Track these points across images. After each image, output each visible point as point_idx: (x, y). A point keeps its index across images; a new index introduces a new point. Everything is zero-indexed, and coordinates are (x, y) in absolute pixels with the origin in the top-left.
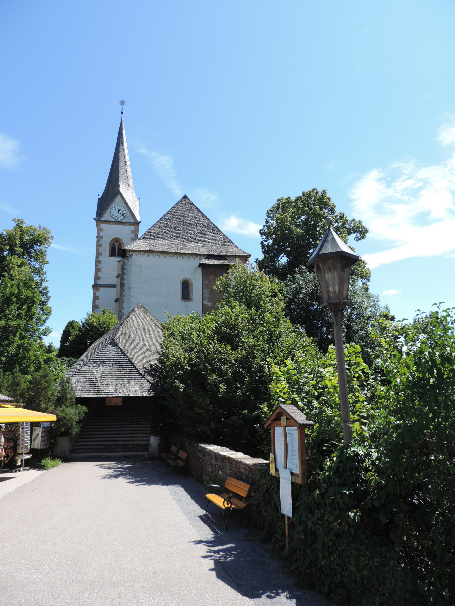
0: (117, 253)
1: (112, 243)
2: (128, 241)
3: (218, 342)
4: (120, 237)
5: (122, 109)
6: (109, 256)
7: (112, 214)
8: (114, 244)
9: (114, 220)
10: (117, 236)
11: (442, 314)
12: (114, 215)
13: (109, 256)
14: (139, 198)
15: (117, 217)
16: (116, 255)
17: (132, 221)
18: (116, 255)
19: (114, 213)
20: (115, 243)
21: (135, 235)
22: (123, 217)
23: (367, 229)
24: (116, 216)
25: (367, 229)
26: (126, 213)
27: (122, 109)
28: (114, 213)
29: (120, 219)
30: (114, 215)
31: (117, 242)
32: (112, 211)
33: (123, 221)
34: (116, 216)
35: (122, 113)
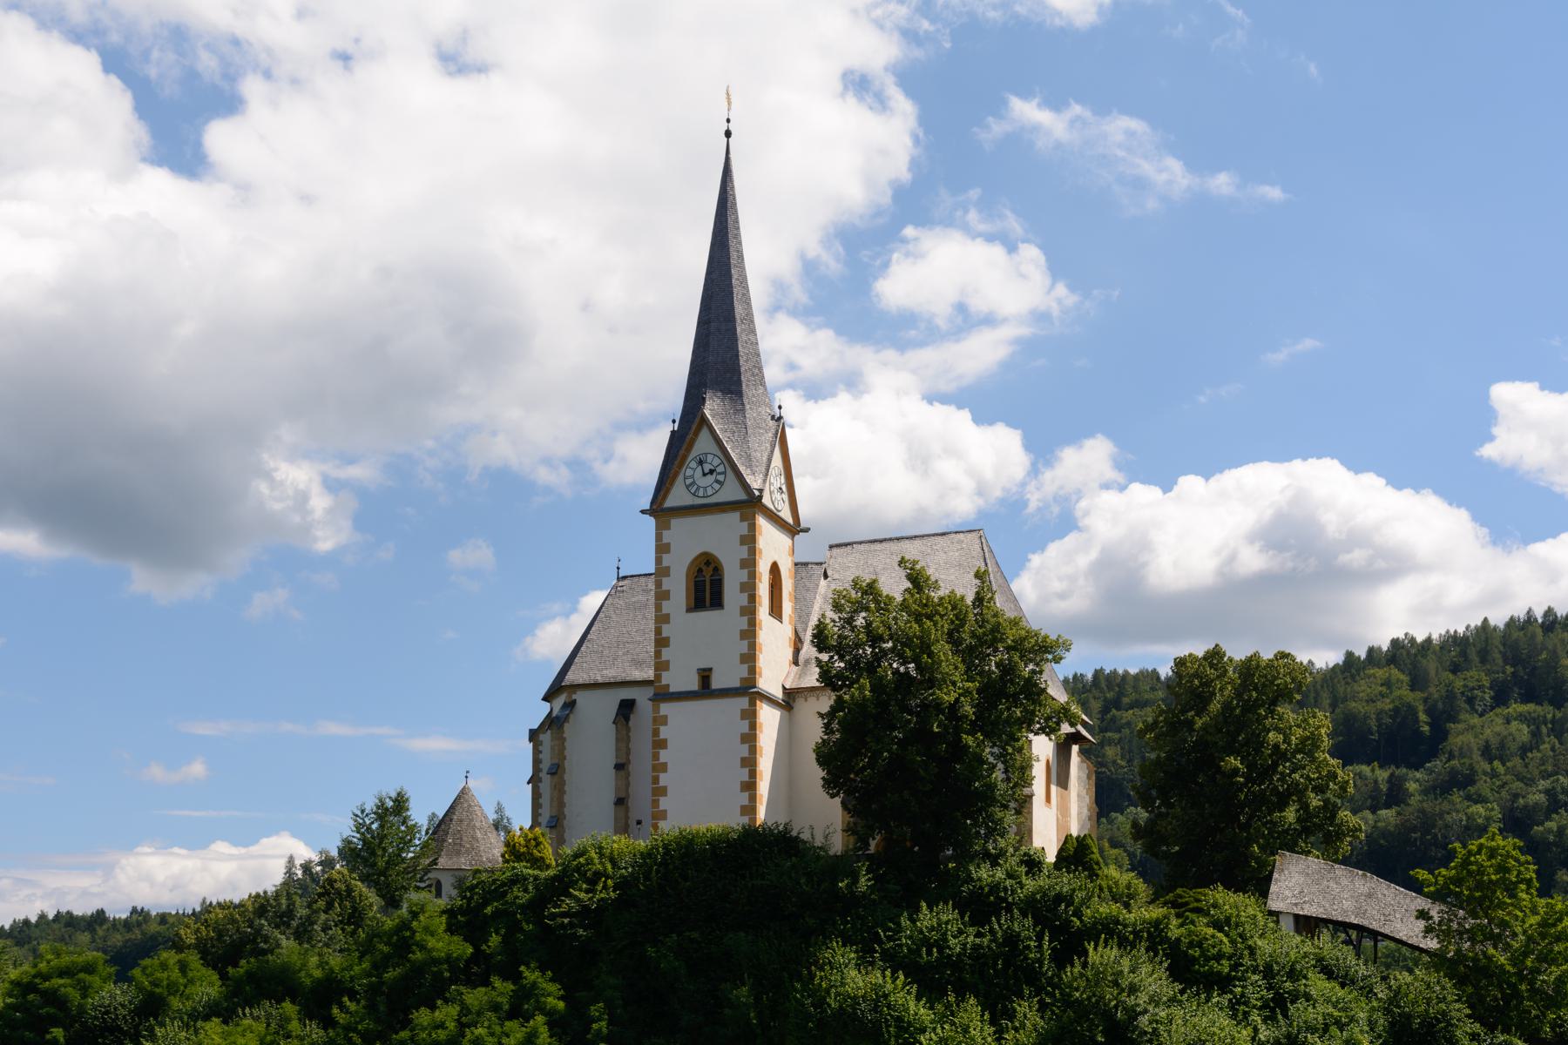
3: (1328, 771)
5: (728, 121)
6: (689, 610)
7: (689, 481)
11: (1480, 753)
12: (694, 483)
13: (689, 610)
14: (780, 407)
15: (701, 489)
19: (692, 477)
22: (717, 486)
23: (142, 909)
24: (698, 488)
25: (142, 909)
26: (724, 473)
27: (728, 121)
28: (692, 477)
30: (694, 483)
31: (708, 563)
32: (689, 472)
35: (728, 134)
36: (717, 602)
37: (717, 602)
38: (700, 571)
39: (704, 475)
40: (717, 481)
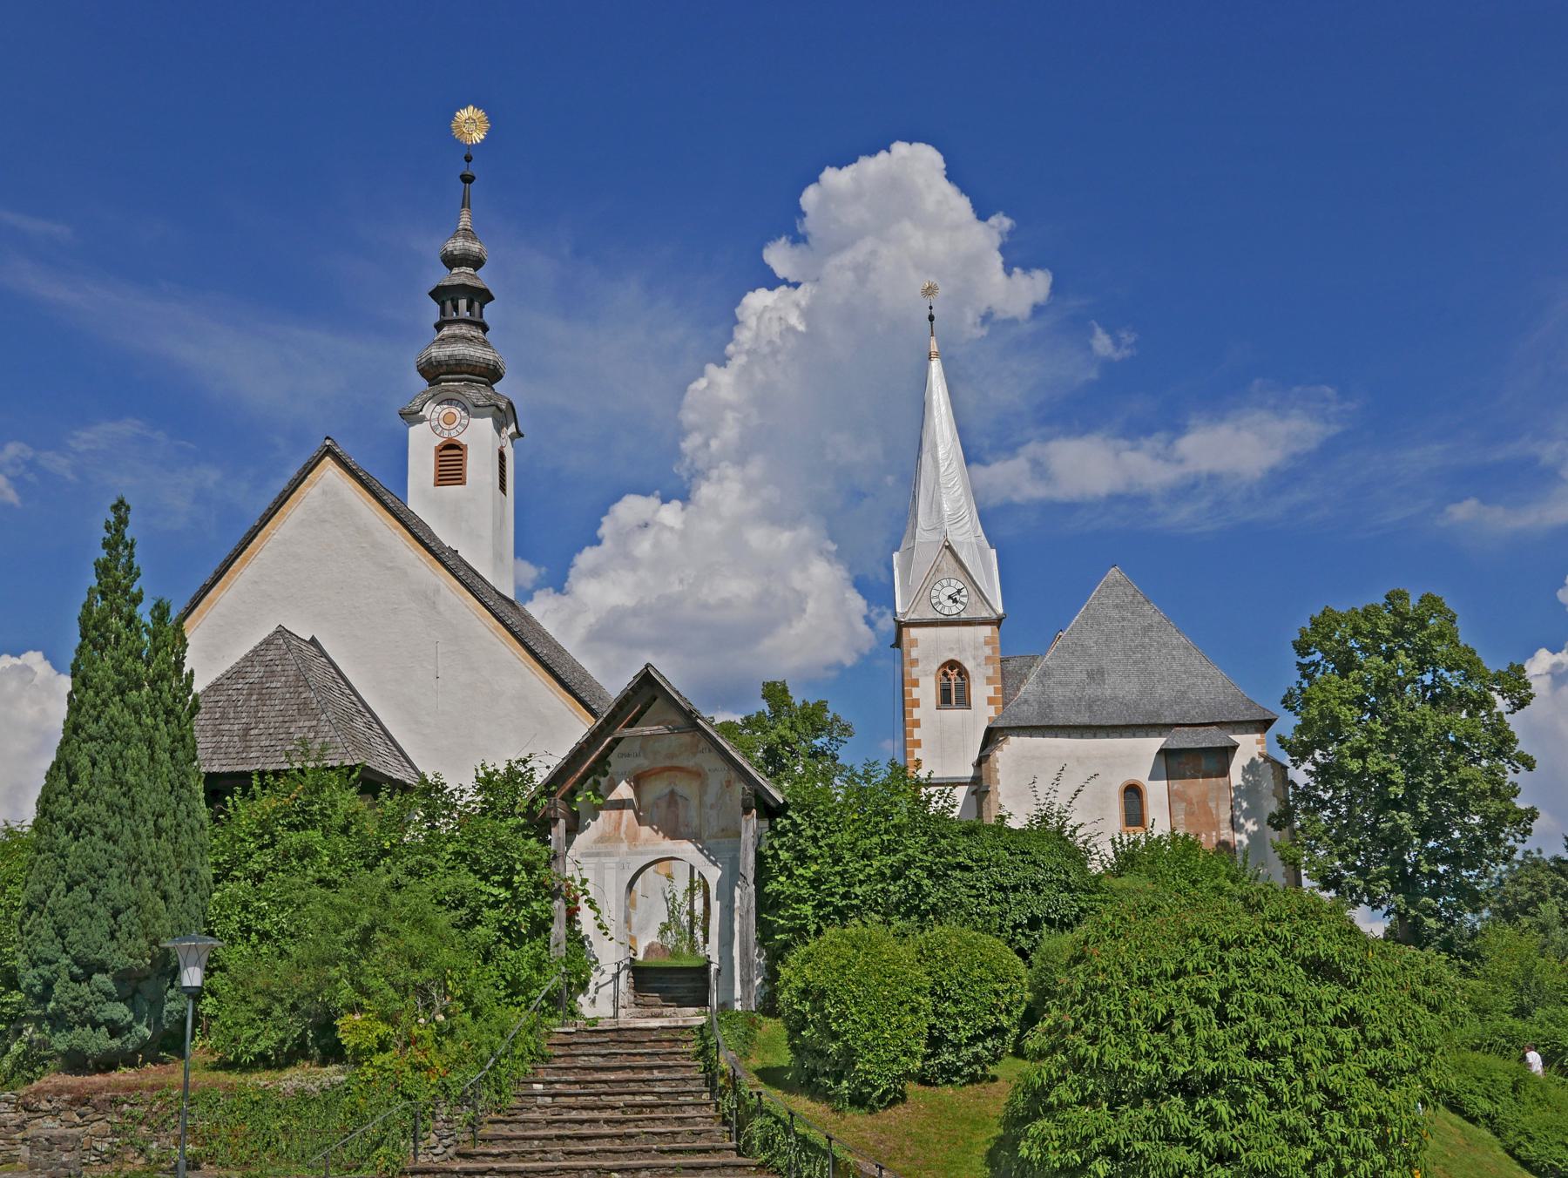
0: (953, 697)
1: (940, 673)
2: (979, 665)
4: (957, 659)
7: (934, 601)
8: (945, 674)
9: (942, 616)
10: (951, 656)
16: (954, 703)
17: (985, 614)
18: (954, 703)
19: (938, 597)
20: (949, 672)
21: (993, 648)
24: (944, 607)
28: (938, 597)
29: (955, 611)
32: (934, 593)
33: (963, 615)
34: (944, 607)
36: (964, 702)
37: (964, 702)
38: (945, 674)
39: (950, 597)
40: (962, 603)
